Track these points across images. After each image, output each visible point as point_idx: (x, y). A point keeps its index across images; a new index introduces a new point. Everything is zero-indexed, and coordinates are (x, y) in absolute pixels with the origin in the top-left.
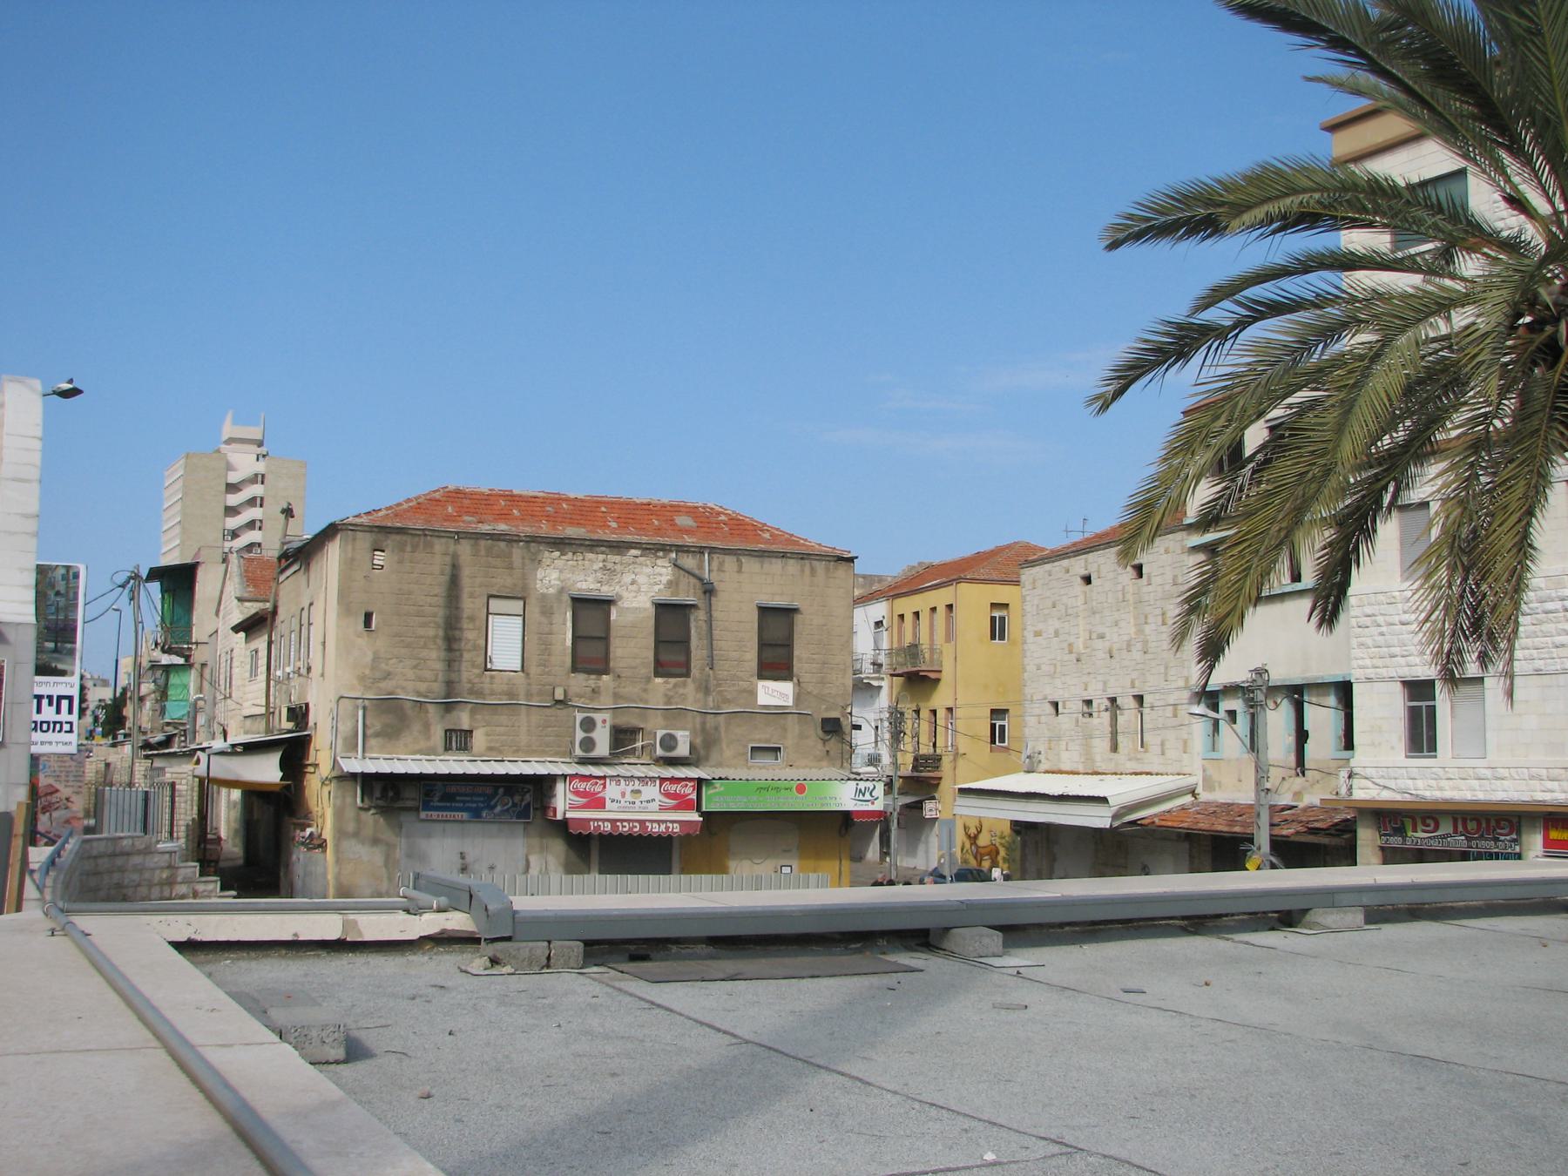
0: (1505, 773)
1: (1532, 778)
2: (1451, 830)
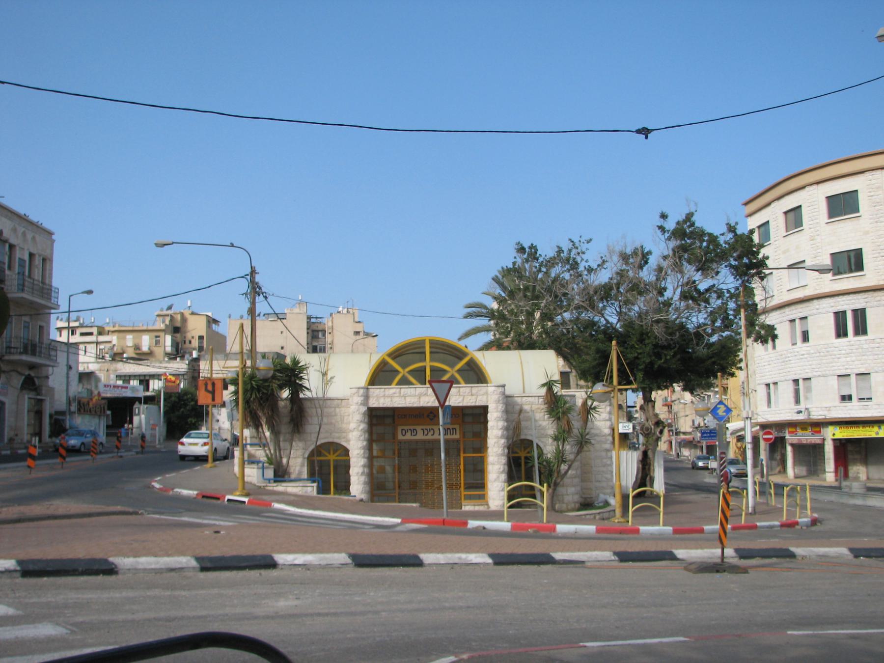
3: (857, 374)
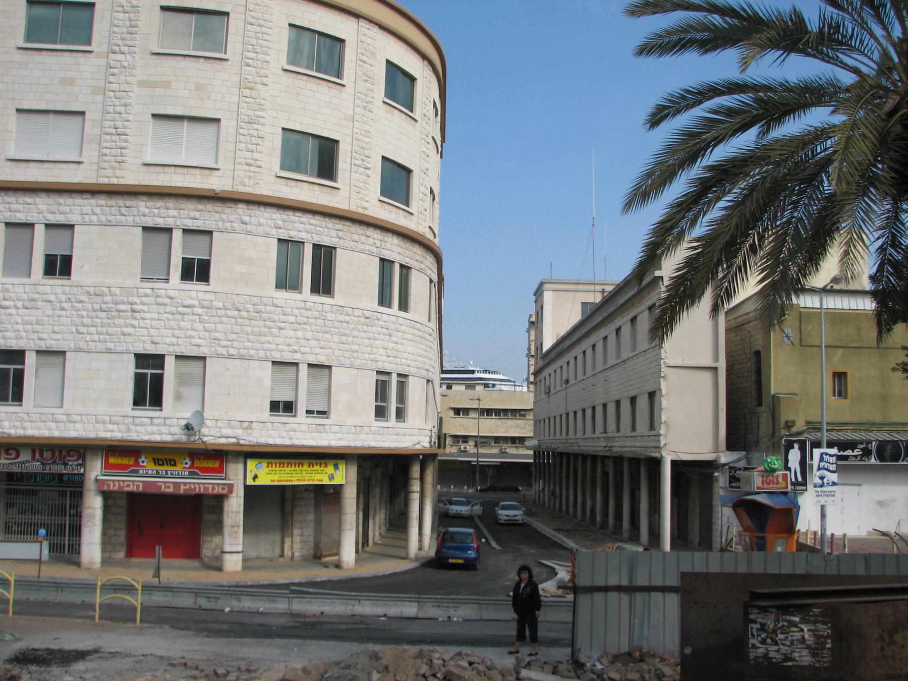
0: (78, 418)
1: (97, 422)
2: (29, 458)
3: (310, 365)
